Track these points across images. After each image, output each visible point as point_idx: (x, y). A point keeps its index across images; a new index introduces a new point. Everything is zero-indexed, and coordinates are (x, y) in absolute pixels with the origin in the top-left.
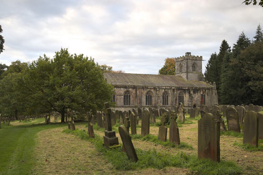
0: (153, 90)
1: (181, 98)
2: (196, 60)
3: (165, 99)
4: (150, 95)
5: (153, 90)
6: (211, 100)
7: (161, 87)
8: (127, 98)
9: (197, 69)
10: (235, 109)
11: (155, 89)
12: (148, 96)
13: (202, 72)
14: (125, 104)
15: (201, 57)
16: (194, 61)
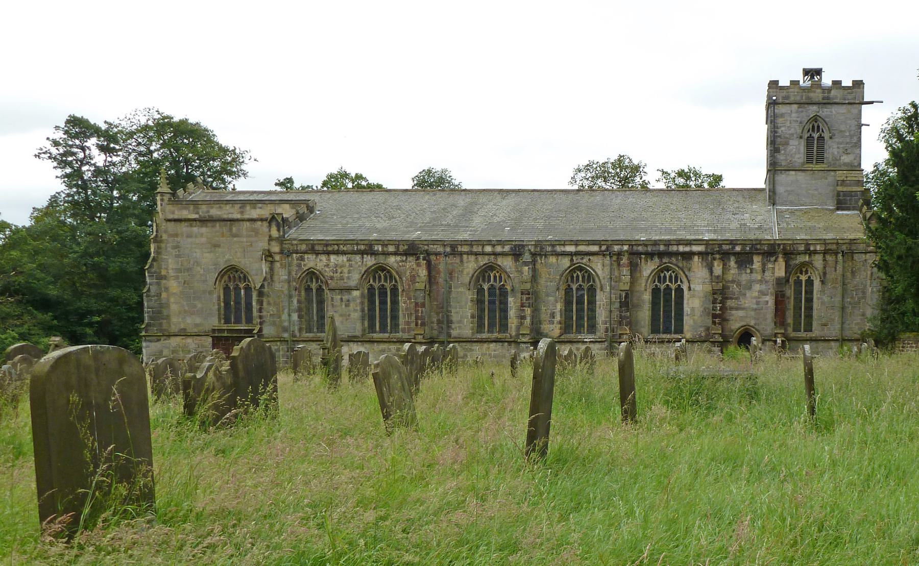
0: (507, 263)
1: (667, 301)
2: (827, 102)
3: (580, 302)
4: (497, 285)
5: (507, 263)
6: (843, 308)
7: (553, 246)
8: (383, 303)
9: (832, 149)
10: (127, 427)
11: (517, 252)
12: (489, 289)
13: (860, 164)
14: (480, 327)
15: (859, 84)
16: (815, 108)
